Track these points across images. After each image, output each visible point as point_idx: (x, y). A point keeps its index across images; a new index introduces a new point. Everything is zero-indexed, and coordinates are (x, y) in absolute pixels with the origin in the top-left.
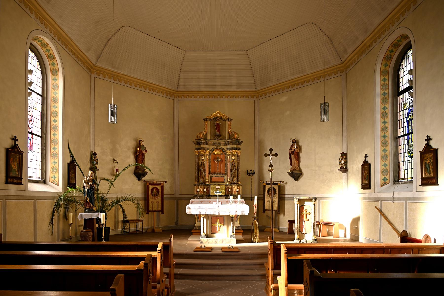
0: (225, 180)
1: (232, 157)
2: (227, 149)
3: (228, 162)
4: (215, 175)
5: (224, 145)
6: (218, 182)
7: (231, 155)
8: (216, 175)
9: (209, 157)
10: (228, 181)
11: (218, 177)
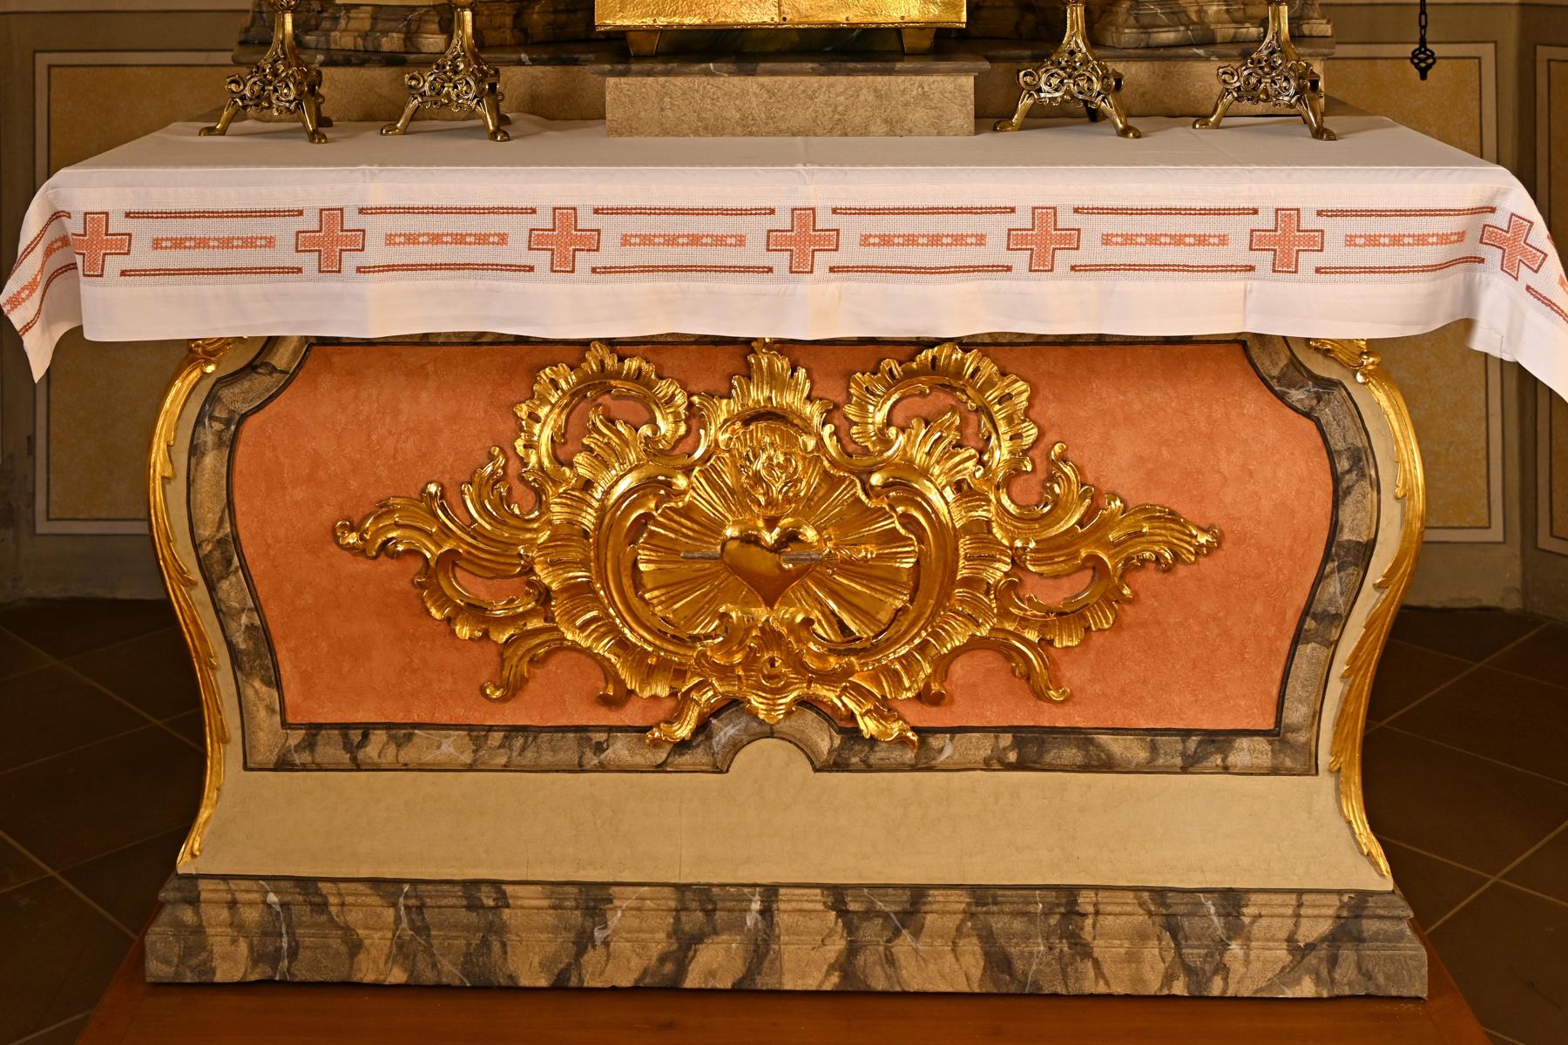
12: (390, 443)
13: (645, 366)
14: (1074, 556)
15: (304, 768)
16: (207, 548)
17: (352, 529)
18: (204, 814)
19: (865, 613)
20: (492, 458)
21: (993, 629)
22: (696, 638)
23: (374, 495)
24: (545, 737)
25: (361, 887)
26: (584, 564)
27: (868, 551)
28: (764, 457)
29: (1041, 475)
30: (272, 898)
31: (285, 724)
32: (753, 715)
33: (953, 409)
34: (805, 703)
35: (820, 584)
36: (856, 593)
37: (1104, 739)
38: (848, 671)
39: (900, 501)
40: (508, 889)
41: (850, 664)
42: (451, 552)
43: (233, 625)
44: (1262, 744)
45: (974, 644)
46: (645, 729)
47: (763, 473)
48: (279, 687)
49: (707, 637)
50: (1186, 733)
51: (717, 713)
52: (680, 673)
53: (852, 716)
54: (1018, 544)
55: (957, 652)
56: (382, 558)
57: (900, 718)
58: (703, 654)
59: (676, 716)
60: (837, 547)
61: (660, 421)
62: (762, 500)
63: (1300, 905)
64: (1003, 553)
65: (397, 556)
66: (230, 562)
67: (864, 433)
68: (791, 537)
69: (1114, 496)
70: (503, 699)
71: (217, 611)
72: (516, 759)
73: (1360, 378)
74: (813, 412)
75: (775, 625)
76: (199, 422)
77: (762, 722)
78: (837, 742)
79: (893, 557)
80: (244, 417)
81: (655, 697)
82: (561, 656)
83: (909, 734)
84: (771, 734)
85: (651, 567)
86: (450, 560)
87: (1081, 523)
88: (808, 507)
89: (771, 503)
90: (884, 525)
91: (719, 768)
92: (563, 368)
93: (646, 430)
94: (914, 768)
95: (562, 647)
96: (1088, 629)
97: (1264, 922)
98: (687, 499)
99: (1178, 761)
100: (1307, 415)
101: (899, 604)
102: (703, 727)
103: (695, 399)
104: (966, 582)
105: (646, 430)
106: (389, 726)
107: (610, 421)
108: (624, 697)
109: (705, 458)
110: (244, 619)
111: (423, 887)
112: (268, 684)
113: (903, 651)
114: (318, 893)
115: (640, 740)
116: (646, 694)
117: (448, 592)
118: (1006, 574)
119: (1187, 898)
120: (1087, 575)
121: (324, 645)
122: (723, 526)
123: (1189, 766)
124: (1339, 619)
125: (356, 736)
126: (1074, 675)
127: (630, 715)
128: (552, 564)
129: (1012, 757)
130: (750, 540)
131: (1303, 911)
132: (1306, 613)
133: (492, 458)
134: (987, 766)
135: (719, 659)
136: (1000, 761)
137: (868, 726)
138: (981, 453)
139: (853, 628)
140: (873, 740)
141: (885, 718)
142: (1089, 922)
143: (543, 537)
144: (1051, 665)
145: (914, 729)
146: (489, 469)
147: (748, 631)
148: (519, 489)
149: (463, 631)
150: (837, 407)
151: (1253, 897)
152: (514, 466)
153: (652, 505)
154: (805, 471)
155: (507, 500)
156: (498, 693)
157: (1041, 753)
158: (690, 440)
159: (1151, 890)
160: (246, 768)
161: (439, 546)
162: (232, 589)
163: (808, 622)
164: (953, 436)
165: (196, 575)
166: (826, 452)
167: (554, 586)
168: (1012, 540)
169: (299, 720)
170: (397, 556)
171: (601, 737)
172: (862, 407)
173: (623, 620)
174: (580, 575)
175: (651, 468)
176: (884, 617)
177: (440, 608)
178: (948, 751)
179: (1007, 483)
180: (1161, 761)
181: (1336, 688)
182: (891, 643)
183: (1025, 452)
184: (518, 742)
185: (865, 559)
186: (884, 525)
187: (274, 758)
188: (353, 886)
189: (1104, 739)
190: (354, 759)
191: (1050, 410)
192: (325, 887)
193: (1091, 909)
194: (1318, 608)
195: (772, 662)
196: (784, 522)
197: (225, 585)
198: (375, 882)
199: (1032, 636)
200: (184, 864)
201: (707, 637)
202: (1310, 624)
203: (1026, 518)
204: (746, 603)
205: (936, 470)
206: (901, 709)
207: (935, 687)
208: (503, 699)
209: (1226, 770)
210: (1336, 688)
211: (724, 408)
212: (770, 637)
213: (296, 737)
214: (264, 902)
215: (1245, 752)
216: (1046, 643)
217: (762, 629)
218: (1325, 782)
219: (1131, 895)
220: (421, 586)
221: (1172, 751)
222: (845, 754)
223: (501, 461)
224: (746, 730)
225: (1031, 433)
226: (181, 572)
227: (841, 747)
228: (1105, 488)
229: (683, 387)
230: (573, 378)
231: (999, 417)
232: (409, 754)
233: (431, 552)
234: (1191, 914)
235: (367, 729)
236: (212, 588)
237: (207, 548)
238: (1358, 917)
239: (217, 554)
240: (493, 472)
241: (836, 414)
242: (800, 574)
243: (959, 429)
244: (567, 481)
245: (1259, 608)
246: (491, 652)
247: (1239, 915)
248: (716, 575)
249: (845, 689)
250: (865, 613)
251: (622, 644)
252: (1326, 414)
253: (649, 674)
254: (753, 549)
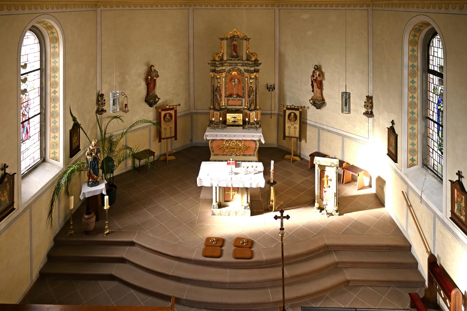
0: (242, 103)
1: (250, 79)
2: (245, 70)
3: (245, 84)
4: (231, 98)
5: (242, 66)
6: (235, 105)
7: (249, 78)
8: (233, 98)
9: (225, 80)
10: (245, 105)
11: (235, 100)
88: (235, 146)
130: (233, 147)
242: (235, 148)
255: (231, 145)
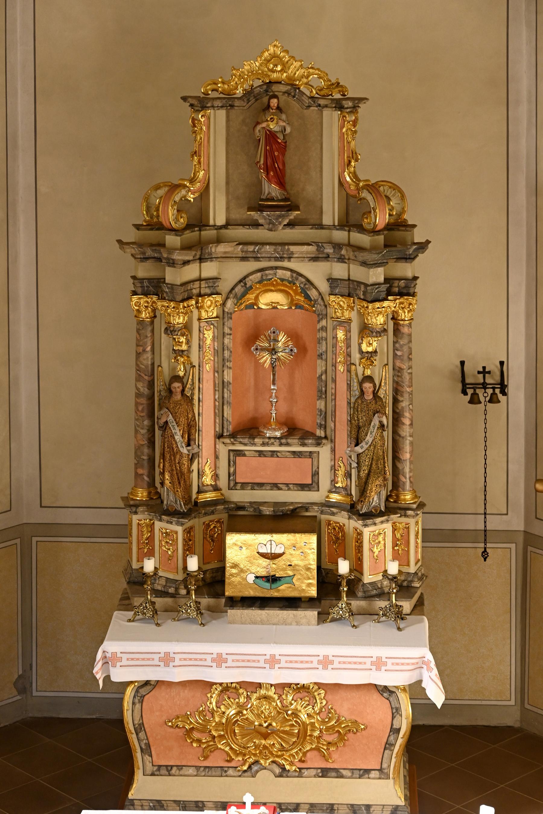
12: (178, 702)
13: (237, 685)
14: (334, 730)
15: (158, 775)
16: (137, 726)
17: (170, 722)
18: (134, 786)
19: (287, 742)
20: (202, 706)
21: (316, 746)
22: (249, 747)
23: (175, 714)
24: (213, 769)
25: (171, 802)
26: (223, 730)
27: (287, 729)
28: (264, 707)
29: (327, 712)
30: (151, 804)
31: (153, 765)
32: (261, 764)
33: (307, 696)
34: (273, 762)
35: (277, 735)
36: (284, 737)
37: (341, 771)
38: (283, 755)
39: (295, 717)
40: (205, 803)
41: (283, 753)
42: (193, 728)
43: (142, 743)
44: (377, 772)
45: (311, 749)
46: (237, 767)
47: (264, 711)
48: (152, 757)
49: (251, 747)
50: (360, 770)
51: (253, 764)
52: (244, 755)
53: (284, 765)
54: (321, 727)
55: (308, 751)
56: (177, 728)
57: (295, 765)
58: (250, 751)
59: (244, 764)
60: (280, 727)
61: (240, 699)
62: (263, 717)
63: (383, 808)
64: (318, 729)
65: (180, 728)
66: (141, 729)
67: (287, 702)
68: (270, 725)
69: (343, 717)
70: (204, 760)
71: (138, 740)
72: (207, 774)
73: (400, 691)
74: (276, 697)
75: (266, 744)
76: (134, 697)
77: (263, 766)
78: (280, 771)
79: (293, 730)
80: (144, 696)
81: (239, 760)
82: (217, 751)
83: (297, 769)
84: (265, 769)
85: (238, 731)
86: (192, 729)
87: (335, 723)
88: (274, 719)
89: (265, 717)
90: (291, 723)
91: (253, 776)
92: (218, 685)
93: (237, 700)
94: (298, 777)
95: (217, 748)
96: (338, 746)
97: (375, 812)
98: (246, 716)
99: (358, 776)
100: (387, 699)
101: (294, 740)
102: (250, 767)
103: (249, 693)
104: (310, 736)
105: (237, 700)
106: (177, 766)
107: (229, 698)
108: (231, 760)
109: (250, 707)
110: (144, 742)
111: (185, 802)
112: (149, 756)
113: (295, 751)
114: (161, 803)
115: (235, 770)
116: (237, 759)
117: (192, 736)
118: (319, 734)
119: (358, 806)
120: (337, 735)
121: (162, 747)
122: (254, 722)
123: (360, 777)
124: (393, 745)
125: (169, 768)
126: (335, 756)
127: (233, 764)
128: (216, 730)
129: (320, 775)
130: (261, 725)
131: (384, 809)
132: (386, 743)
133: (202, 706)
134: (315, 776)
135: (253, 752)
136: (318, 776)
137: (288, 767)
138: (313, 707)
139: (284, 745)
140: (289, 770)
141: (292, 766)
142: (336, 811)
143: (214, 724)
144: (329, 754)
145: (298, 768)
146: (201, 709)
147: (260, 746)
148: (208, 713)
149: (195, 745)
150: (281, 696)
151: (373, 806)
152: (207, 708)
153: (238, 718)
154: (273, 710)
155: (205, 716)
156: (202, 759)
157: (327, 774)
158: (247, 703)
159: (350, 804)
160: (144, 775)
161: (190, 726)
162: (142, 735)
163: (274, 744)
164: (307, 703)
165: (133, 731)
166: (278, 706)
167: (216, 735)
168: (320, 726)
169: (156, 764)
170: (180, 728)
171: (226, 769)
172: (287, 695)
173: (232, 743)
174: (222, 733)
175: (238, 709)
176: (291, 743)
177: (190, 739)
178: (306, 773)
179: (319, 714)
180: (354, 776)
181: (394, 760)
182: (292, 749)
183: (323, 707)
184: (207, 770)
185: (287, 730)
186: (291, 723)
187: (150, 773)
188: (169, 802)
189: (341, 771)
190: (169, 773)
191: (329, 697)
192: (163, 802)
193: (336, 809)
194: (389, 742)
195: (266, 753)
196: (269, 722)
197: (140, 734)
198: (175, 801)
199: (325, 748)
200: (130, 796)
201: (251, 747)
202: (387, 746)
203: (323, 722)
204: (260, 739)
205: (303, 711)
206: (295, 763)
207: (303, 759)
208: (204, 760)
209: (369, 778)
210: (394, 760)
211: (255, 696)
212: (265, 747)
213: (155, 768)
214: (149, 805)
215: (373, 774)
216: (328, 749)
217: (263, 746)
218: (391, 781)
219: (346, 805)
220: (185, 735)
221: (357, 773)
222: (282, 774)
223: (204, 707)
224: (259, 768)
225: (324, 702)
226: (130, 731)
227: (281, 772)
228: (341, 715)
229: (246, 690)
230: (221, 688)
231: (317, 699)
232: (182, 772)
233: (187, 727)
234: (359, 810)
235: (172, 767)
236: (137, 734)
237: (137, 726)
238: (396, 811)
239: (139, 727)
240: (202, 710)
241: (281, 697)
242: (272, 733)
243: (309, 701)
244: (219, 712)
245: (376, 742)
246: (201, 749)
247: (370, 810)
248: (253, 733)
249: (282, 759)
250: (287, 742)
251: (231, 748)
252: (391, 699)
253: (237, 755)
254: (261, 727)
255: (251, 716)
